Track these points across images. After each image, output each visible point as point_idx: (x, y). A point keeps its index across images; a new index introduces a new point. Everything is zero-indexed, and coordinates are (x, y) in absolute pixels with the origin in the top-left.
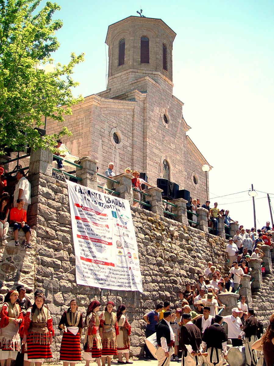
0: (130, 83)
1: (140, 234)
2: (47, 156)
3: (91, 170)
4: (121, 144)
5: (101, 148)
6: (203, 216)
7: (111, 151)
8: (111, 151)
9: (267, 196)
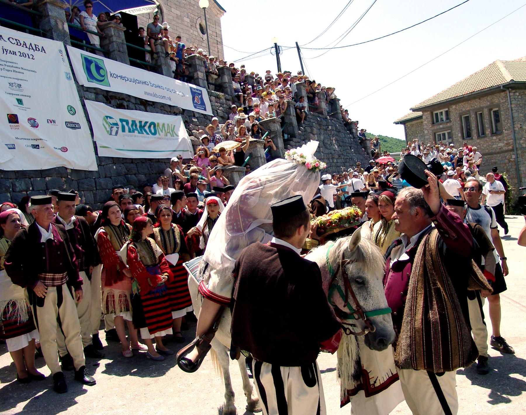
1: (87, 92)
6: (198, 66)
9: (296, 46)
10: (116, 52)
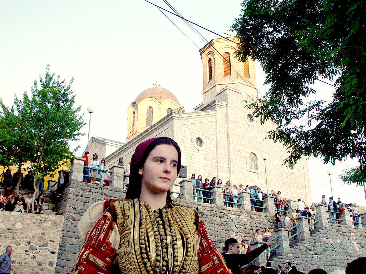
0: (216, 95)
2: (79, 168)
3: (118, 173)
4: (204, 146)
5: (184, 152)
6: (244, 197)
7: (193, 153)
8: (193, 153)
10: (186, 194)
